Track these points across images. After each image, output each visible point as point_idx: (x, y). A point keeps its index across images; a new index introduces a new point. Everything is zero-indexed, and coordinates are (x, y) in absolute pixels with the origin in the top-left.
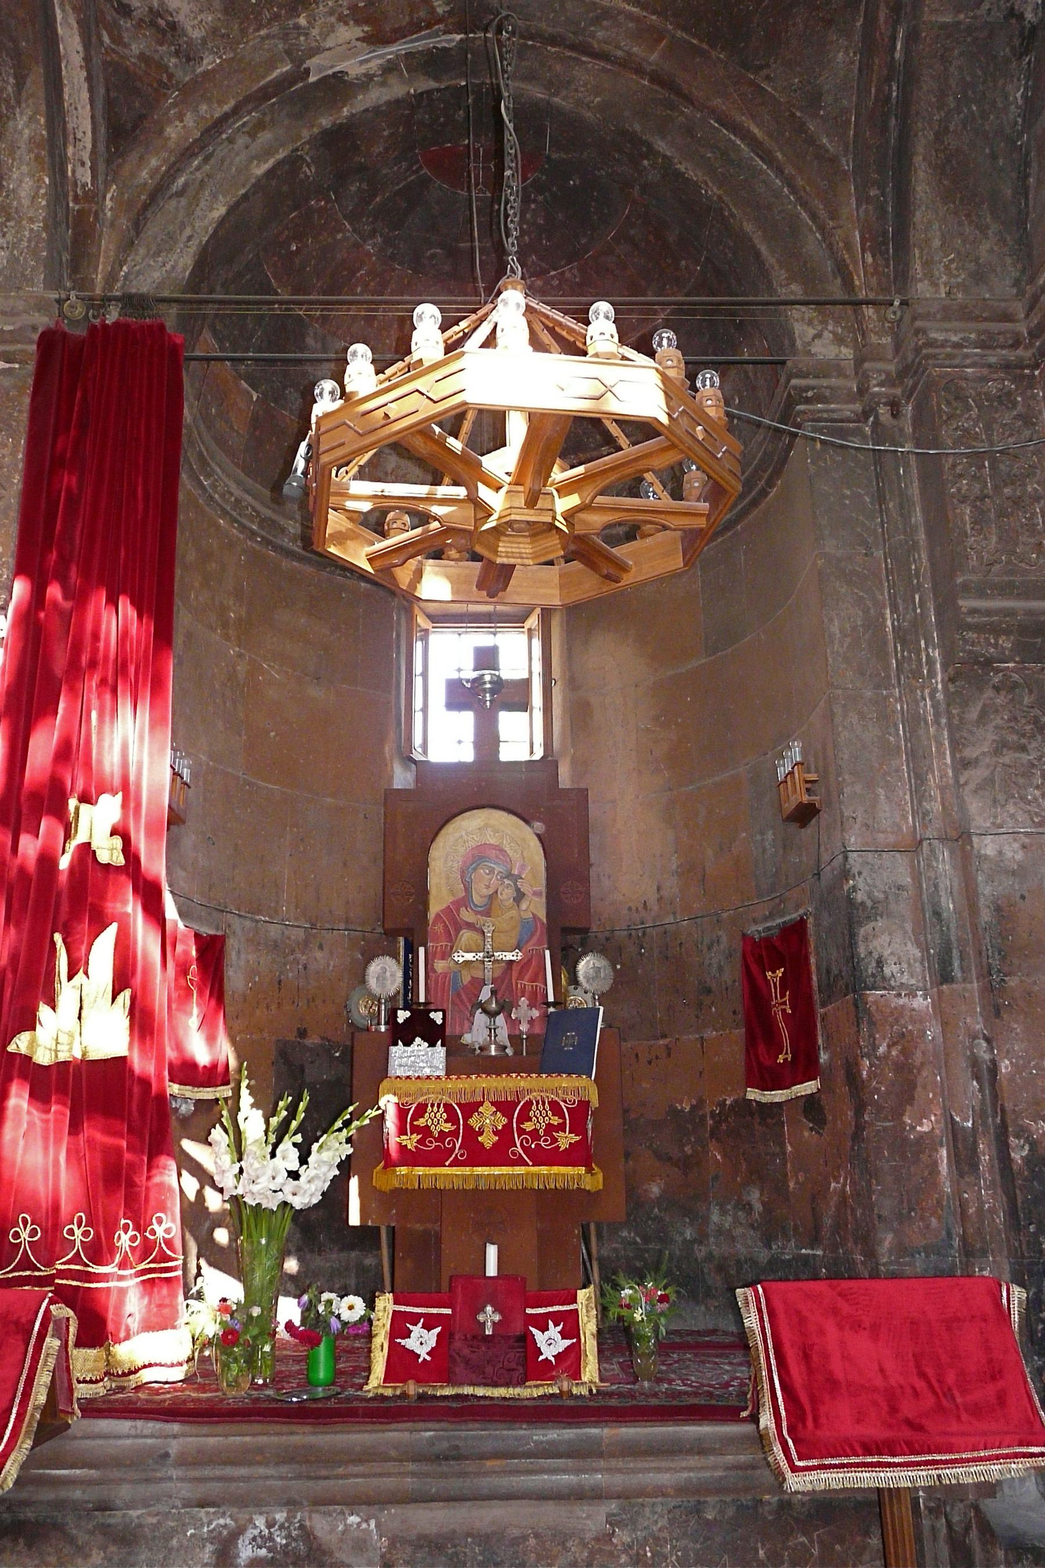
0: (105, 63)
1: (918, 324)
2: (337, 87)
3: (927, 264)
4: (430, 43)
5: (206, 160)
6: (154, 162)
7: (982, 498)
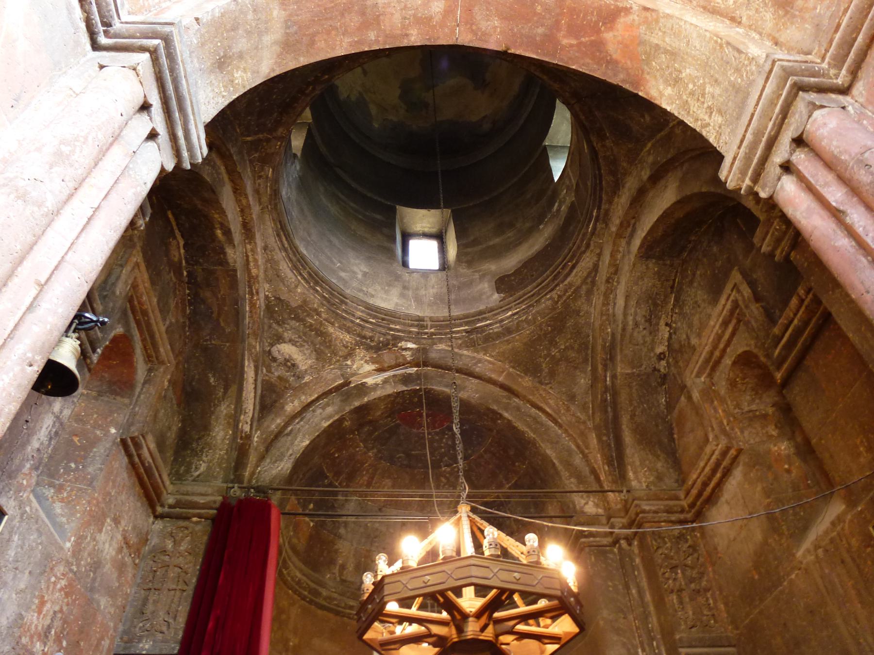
0: (263, 381)
1: (636, 502)
2: (362, 389)
3: (635, 473)
4: (403, 371)
5: (301, 420)
6: (278, 421)
7: (680, 590)
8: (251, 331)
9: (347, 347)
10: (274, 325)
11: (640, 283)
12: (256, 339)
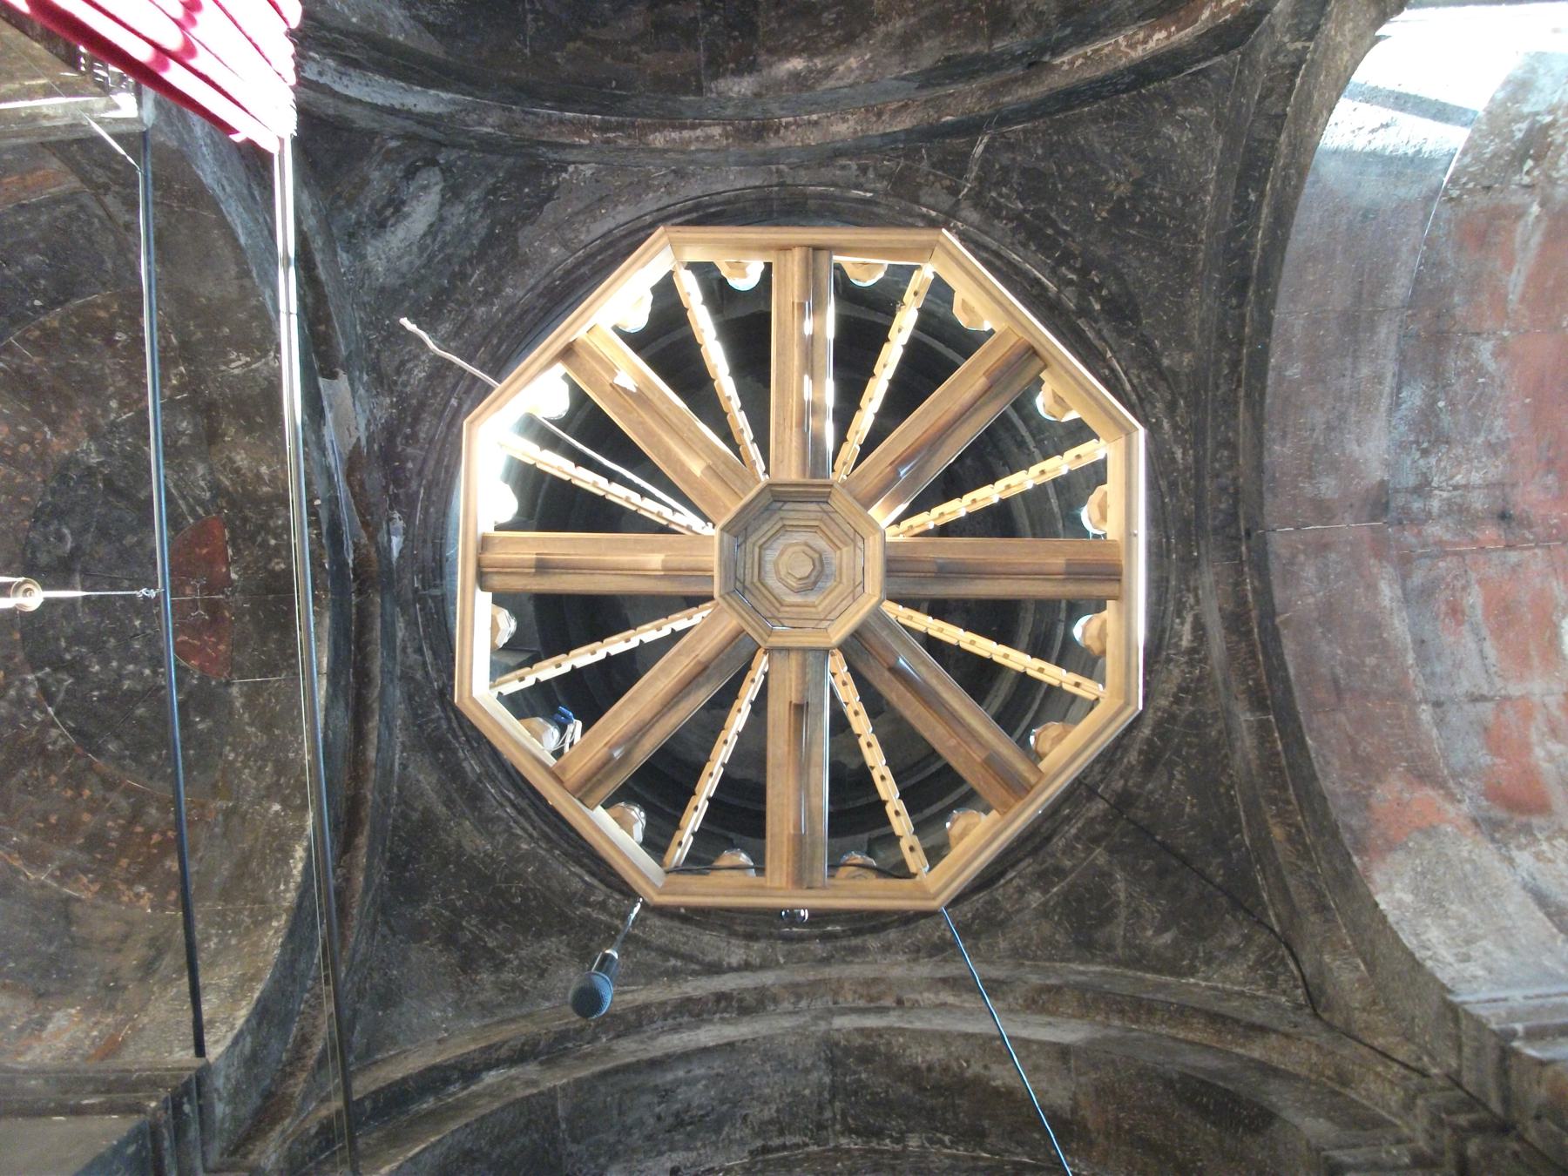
8: (518, 116)
9: (398, 372)
10: (491, 181)
11: (768, 1068)
12: (500, 127)
